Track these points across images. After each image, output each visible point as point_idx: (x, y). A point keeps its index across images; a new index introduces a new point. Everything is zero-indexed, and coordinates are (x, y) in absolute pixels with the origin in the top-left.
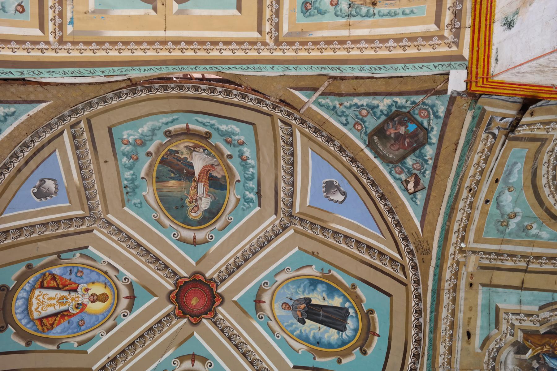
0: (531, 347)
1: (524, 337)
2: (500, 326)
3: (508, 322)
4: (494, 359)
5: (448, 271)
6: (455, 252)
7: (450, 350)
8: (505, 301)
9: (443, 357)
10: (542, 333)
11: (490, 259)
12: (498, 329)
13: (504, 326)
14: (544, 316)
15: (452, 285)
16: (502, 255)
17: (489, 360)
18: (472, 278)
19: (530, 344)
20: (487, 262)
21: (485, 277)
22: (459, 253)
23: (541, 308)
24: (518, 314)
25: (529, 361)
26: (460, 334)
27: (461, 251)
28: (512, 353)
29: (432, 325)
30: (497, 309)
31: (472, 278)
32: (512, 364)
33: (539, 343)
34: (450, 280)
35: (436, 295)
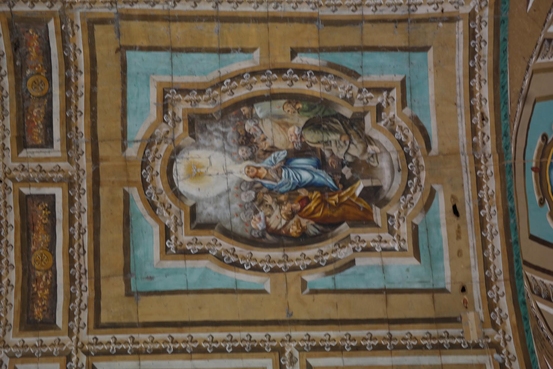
0: (358, 200)
1: (372, 214)
2: (410, 230)
3: (399, 236)
4: (410, 176)
5: (506, 311)
6: (506, 344)
7: (479, 184)
8: (408, 270)
9: (489, 172)
10: (345, 225)
11: (448, 337)
12: (413, 224)
13: (404, 230)
14: (345, 250)
15: (494, 287)
16: (434, 347)
17: (419, 173)
18: (465, 301)
19: (360, 204)
20: (451, 332)
21: (447, 305)
22: (499, 343)
23: (351, 263)
24: (384, 250)
25: (356, 176)
26: (468, 209)
27: (495, 347)
28: (386, 187)
29: (512, 221)
30: (417, 255)
31: (465, 301)
32: (382, 169)
33: (347, 207)
34: (498, 296)
35: (516, 270)
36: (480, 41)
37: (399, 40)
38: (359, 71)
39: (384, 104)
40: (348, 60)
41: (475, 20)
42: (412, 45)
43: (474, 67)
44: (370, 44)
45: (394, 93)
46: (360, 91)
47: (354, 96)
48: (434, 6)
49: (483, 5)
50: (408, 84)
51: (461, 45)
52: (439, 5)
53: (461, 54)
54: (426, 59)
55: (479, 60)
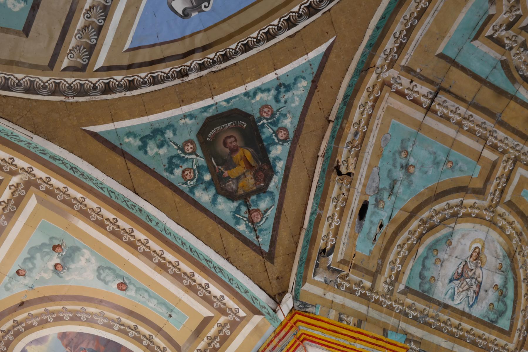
36: (398, 38)
37: (456, 74)
38: (499, 66)
39: (504, 27)
40: (500, 79)
41: (392, 59)
42: (449, 65)
43: (415, 18)
44: (476, 82)
45: (489, 32)
46: (511, 48)
47: (518, 47)
48: (415, 89)
49: (380, 69)
50: (474, 34)
51: (413, 43)
52: (411, 88)
53: (418, 36)
54: (446, 47)
55: (408, 21)
